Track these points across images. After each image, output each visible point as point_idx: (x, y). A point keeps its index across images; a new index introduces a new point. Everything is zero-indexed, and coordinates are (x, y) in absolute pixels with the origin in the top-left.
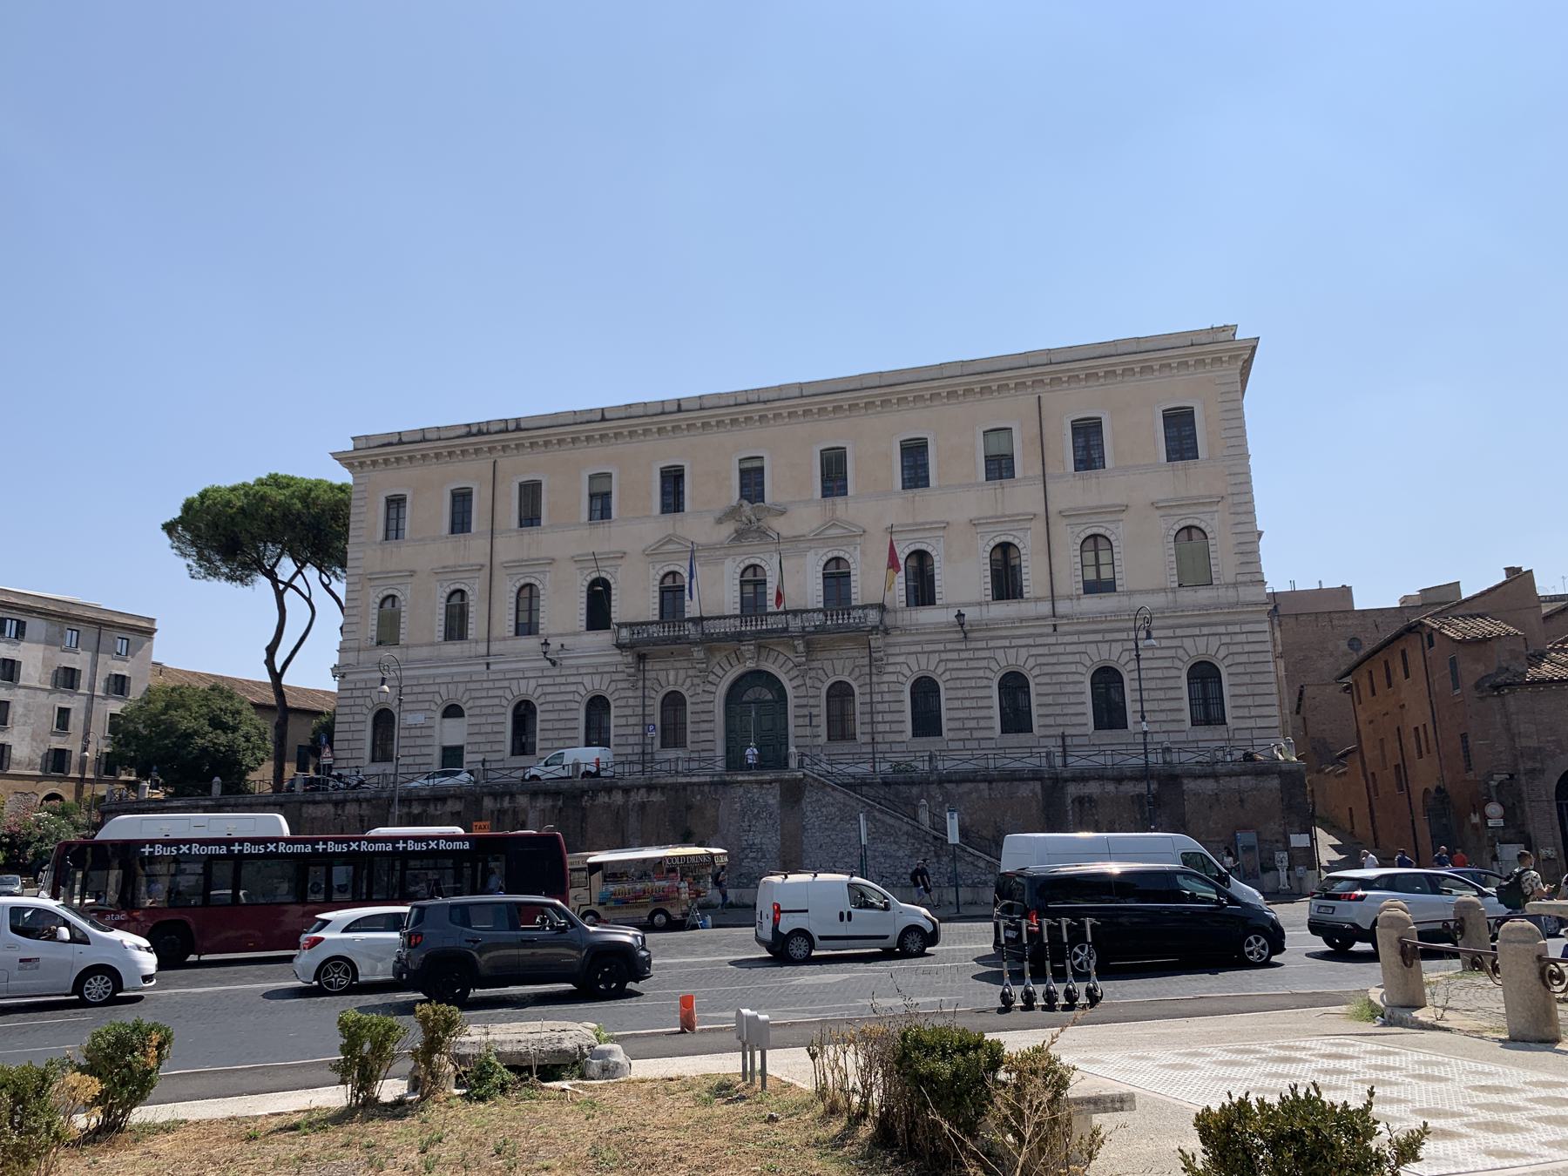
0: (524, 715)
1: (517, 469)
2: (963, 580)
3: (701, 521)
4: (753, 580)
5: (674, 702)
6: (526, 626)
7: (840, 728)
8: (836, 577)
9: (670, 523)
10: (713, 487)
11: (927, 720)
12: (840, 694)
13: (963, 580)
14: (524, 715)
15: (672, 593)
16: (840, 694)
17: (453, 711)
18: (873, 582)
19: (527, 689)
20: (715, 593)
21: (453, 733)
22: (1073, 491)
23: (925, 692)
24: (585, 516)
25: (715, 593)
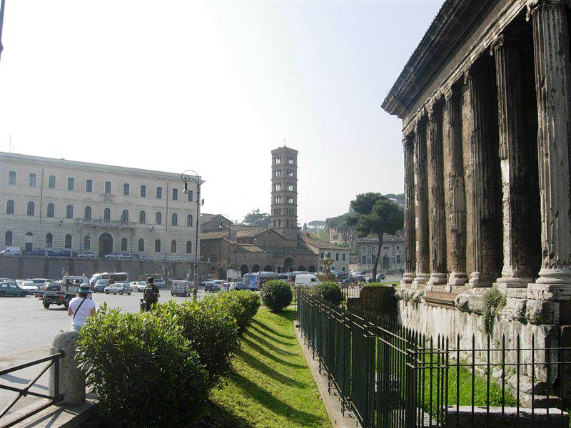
0: (49, 237)
1: (49, 172)
2: (151, 218)
3: (96, 195)
4: (107, 211)
5: (87, 238)
6: (51, 214)
7: (124, 247)
8: (125, 213)
9: (88, 194)
10: (98, 188)
11: (141, 248)
12: (124, 240)
13: (151, 218)
14: (49, 237)
15: (88, 210)
16: (124, 240)
17: (30, 234)
18: (134, 217)
19: (51, 231)
20: (97, 214)
21: (29, 239)
22: (173, 204)
23: (141, 242)
24: (67, 188)
25: (97, 214)
